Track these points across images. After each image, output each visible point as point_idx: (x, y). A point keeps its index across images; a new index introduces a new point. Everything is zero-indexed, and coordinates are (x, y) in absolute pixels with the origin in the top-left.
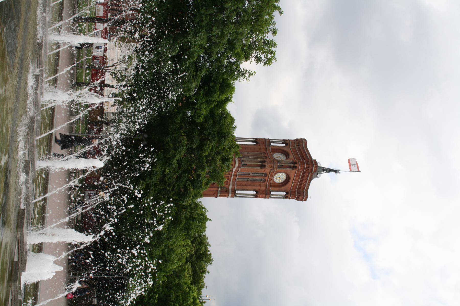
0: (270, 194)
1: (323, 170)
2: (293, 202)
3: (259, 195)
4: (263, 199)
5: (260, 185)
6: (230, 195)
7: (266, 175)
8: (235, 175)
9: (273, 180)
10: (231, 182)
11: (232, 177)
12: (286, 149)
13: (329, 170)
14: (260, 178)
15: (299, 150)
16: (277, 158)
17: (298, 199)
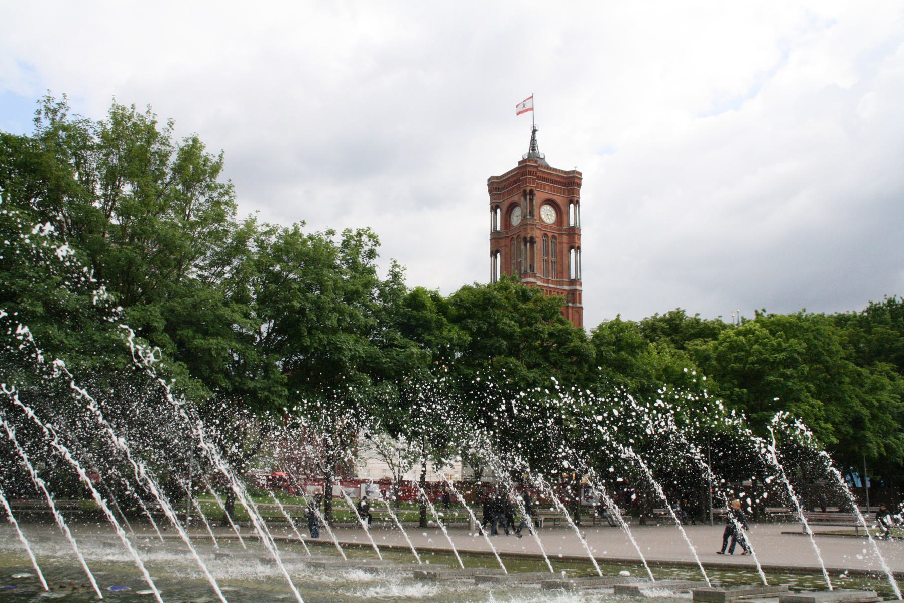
0: (573, 228)
1: (534, 150)
3: (577, 245)
5: (561, 243)
6: (578, 288)
7: (546, 235)
8: (548, 281)
9: (552, 224)
10: (558, 287)
11: (551, 286)
12: (505, 208)
13: (533, 140)
14: (550, 243)
15: (505, 187)
16: (520, 220)
17: (579, 185)
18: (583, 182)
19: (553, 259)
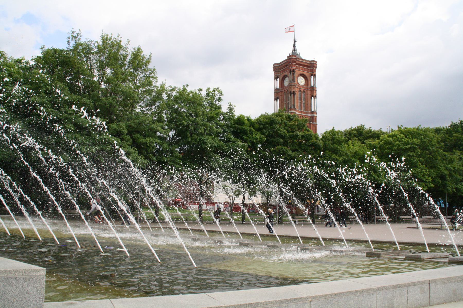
0: (313, 87)
1: (294, 51)
2: (318, 71)
3: (315, 95)
4: (317, 92)
5: (307, 94)
6: (315, 115)
7: (300, 91)
8: (301, 112)
10: (306, 115)
11: (302, 114)
12: (281, 77)
13: (294, 46)
14: (302, 94)
15: (281, 68)
16: (288, 84)
17: (316, 67)
18: (318, 66)
19: (304, 102)
